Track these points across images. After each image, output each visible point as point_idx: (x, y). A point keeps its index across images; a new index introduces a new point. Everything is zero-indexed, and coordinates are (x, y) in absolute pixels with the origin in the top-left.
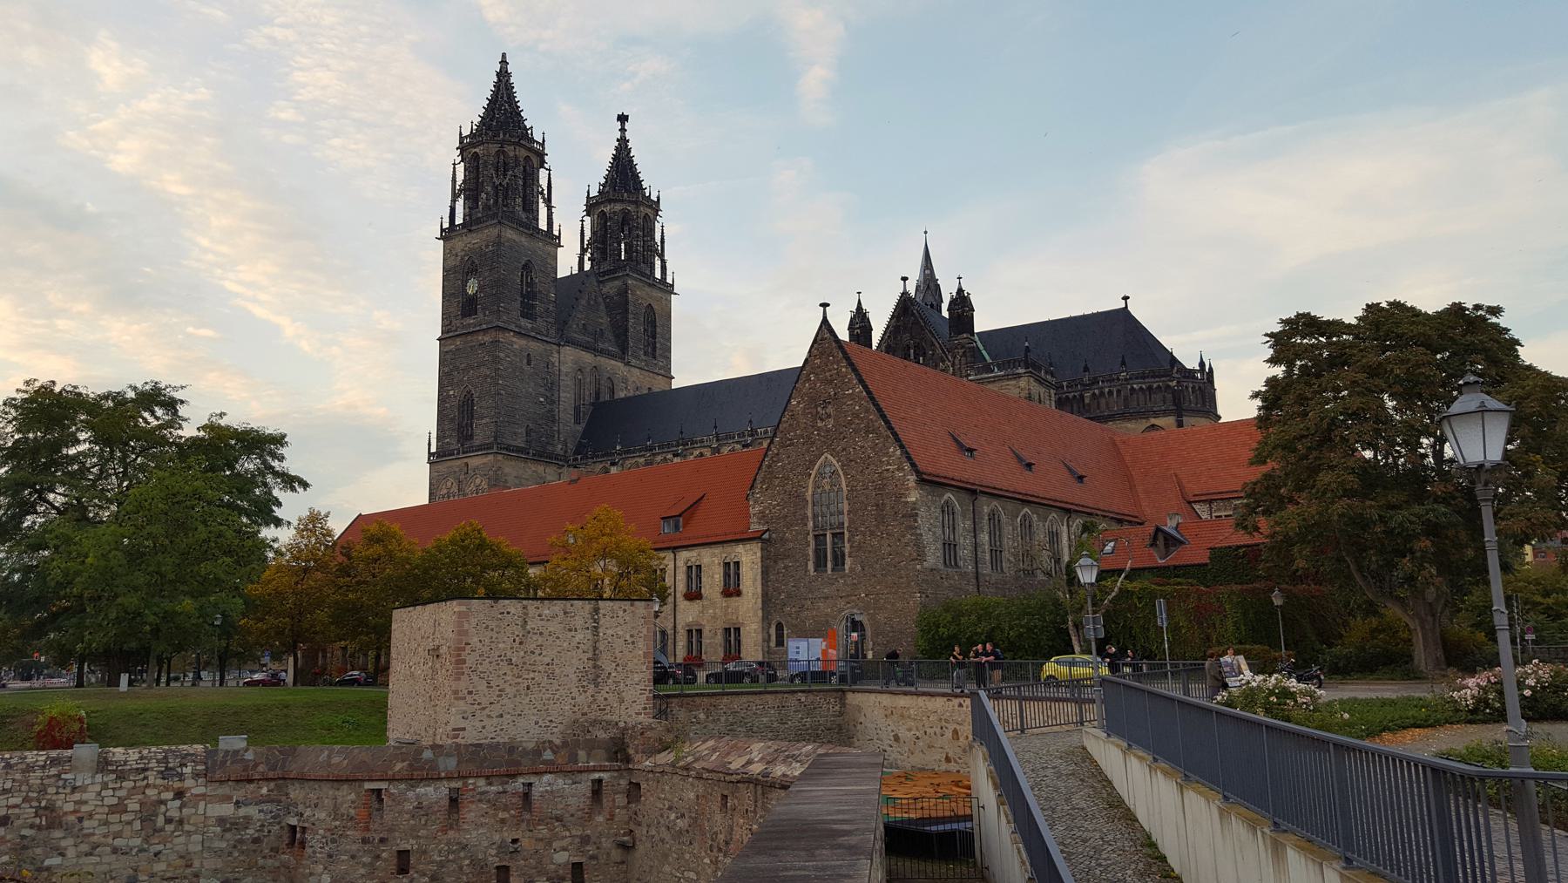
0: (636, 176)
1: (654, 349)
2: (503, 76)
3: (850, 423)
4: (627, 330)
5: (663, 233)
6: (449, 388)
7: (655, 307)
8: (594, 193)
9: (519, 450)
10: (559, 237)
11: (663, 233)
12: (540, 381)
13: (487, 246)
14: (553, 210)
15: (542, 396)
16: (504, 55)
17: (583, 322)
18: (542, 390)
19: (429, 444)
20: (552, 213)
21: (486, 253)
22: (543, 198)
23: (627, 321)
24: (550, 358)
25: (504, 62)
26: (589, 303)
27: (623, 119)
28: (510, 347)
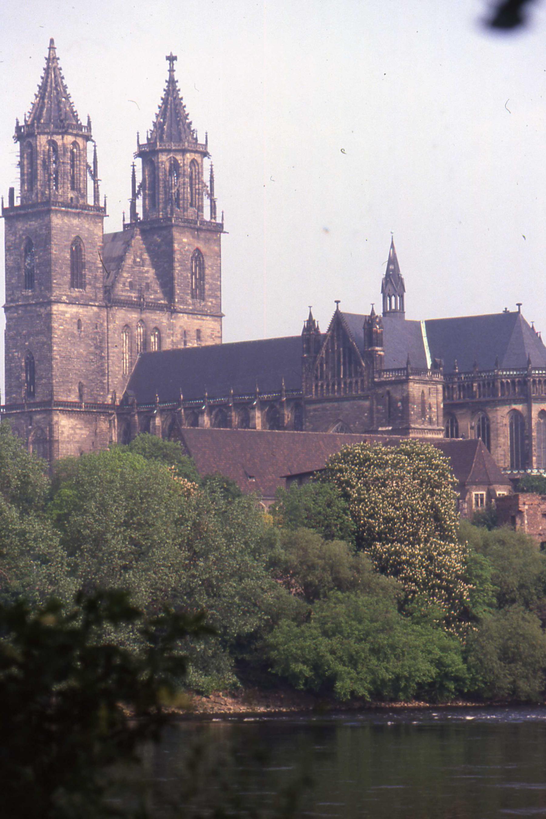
1: (202, 290)
2: (52, 60)
4: (172, 279)
5: (212, 172)
6: (14, 350)
8: (143, 141)
9: (73, 404)
10: (105, 208)
11: (212, 172)
13: (41, 229)
14: (99, 183)
16: (52, 41)
17: (129, 280)
20: (98, 186)
22: (91, 172)
23: (172, 268)
25: (52, 48)
26: (134, 261)
27: (172, 59)
28: (62, 317)
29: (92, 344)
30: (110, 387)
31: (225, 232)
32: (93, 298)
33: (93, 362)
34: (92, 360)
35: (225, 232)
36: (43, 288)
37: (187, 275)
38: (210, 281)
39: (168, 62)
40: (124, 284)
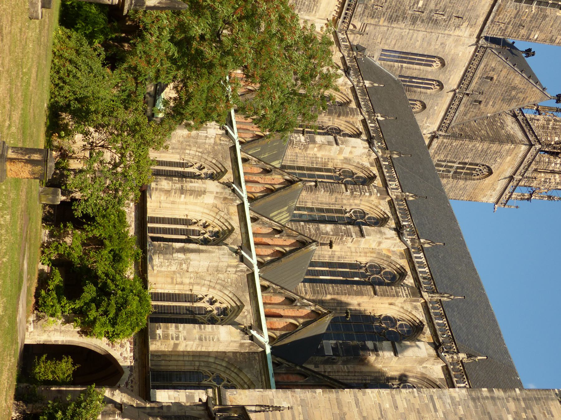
4: (471, 139)
7: (488, 180)
12: (442, 4)
15: (425, 5)
17: (495, 78)
18: (432, 6)
24: (466, 23)
26: (514, 88)
29: (438, 6)
30: (372, 27)
32: (497, 19)
33: (414, 5)
34: (418, 3)
37: (468, 158)
38: (449, 186)
40: (494, 70)
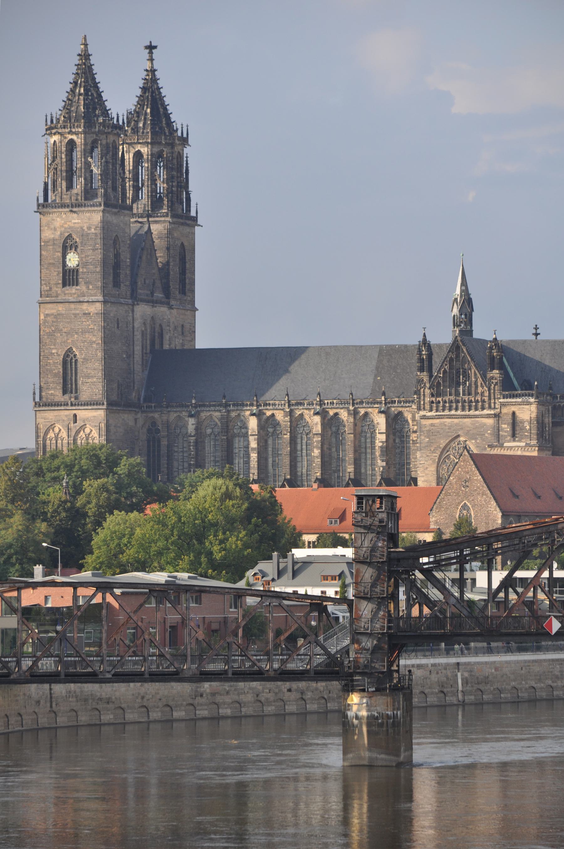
0: (167, 116)
2: (85, 56)
3: (476, 490)
13: (89, 228)
19: (34, 394)
21: (88, 235)
27: (151, 48)
31: (199, 225)
35: (199, 225)
36: (91, 287)
39: (148, 51)
